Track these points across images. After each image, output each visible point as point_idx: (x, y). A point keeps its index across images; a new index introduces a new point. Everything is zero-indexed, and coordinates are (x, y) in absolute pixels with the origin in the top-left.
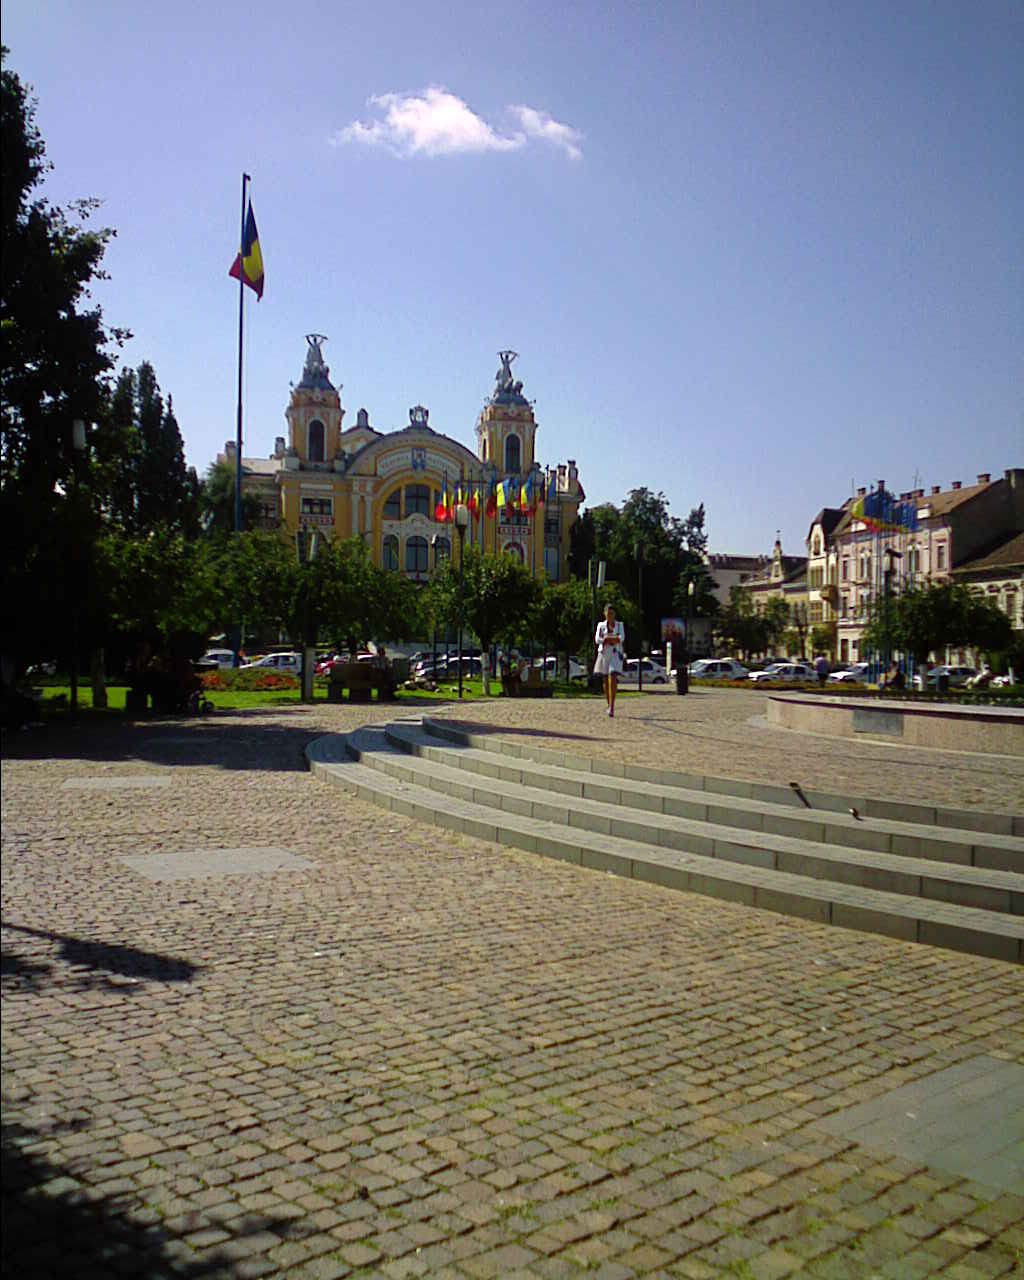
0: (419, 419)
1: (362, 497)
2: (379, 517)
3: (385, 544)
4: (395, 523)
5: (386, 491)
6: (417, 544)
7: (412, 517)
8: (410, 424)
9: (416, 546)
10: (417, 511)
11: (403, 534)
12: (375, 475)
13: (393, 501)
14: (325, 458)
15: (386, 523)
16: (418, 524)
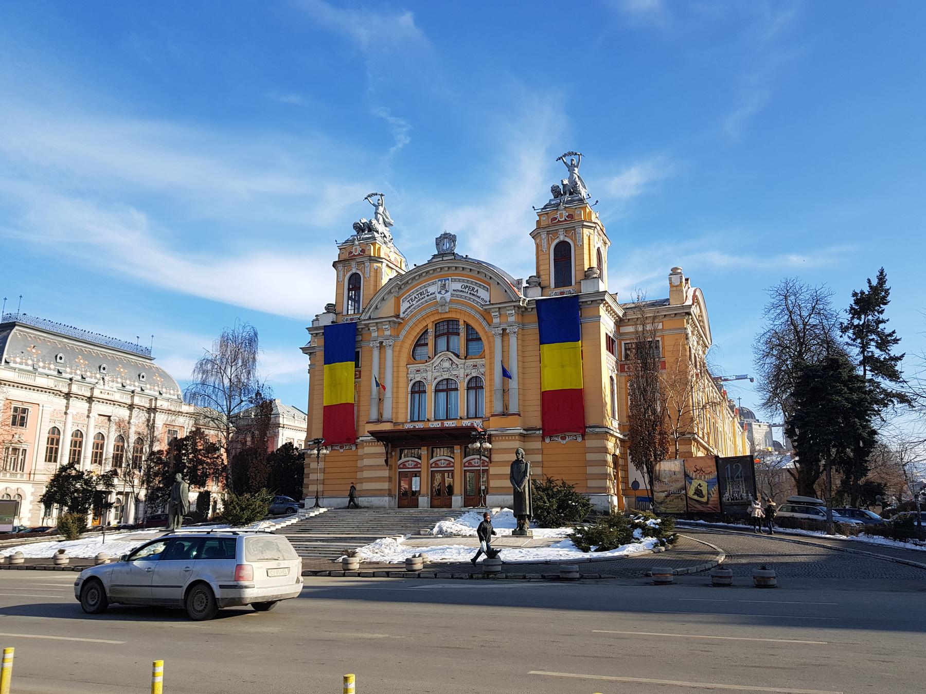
0: (447, 245)
1: (381, 343)
2: (403, 362)
3: (413, 393)
4: (422, 367)
5: (409, 336)
6: (446, 387)
7: (437, 360)
8: (436, 253)
9: (447, 390)
10: (448, 350)
11: (429, 376)
12: (398, 316)
13: (420, 343)
14: (361, 312)
15: (412, 368)
16: (447, 364)
